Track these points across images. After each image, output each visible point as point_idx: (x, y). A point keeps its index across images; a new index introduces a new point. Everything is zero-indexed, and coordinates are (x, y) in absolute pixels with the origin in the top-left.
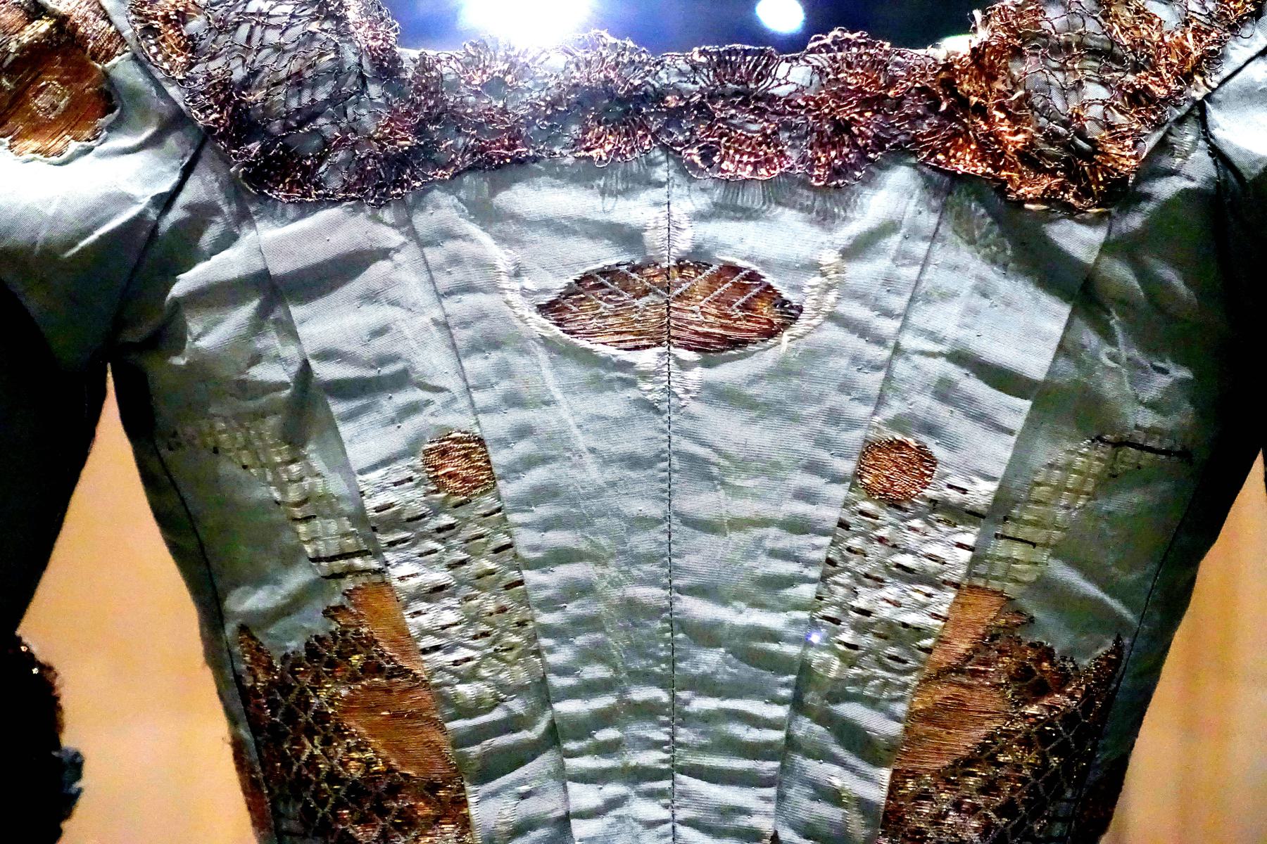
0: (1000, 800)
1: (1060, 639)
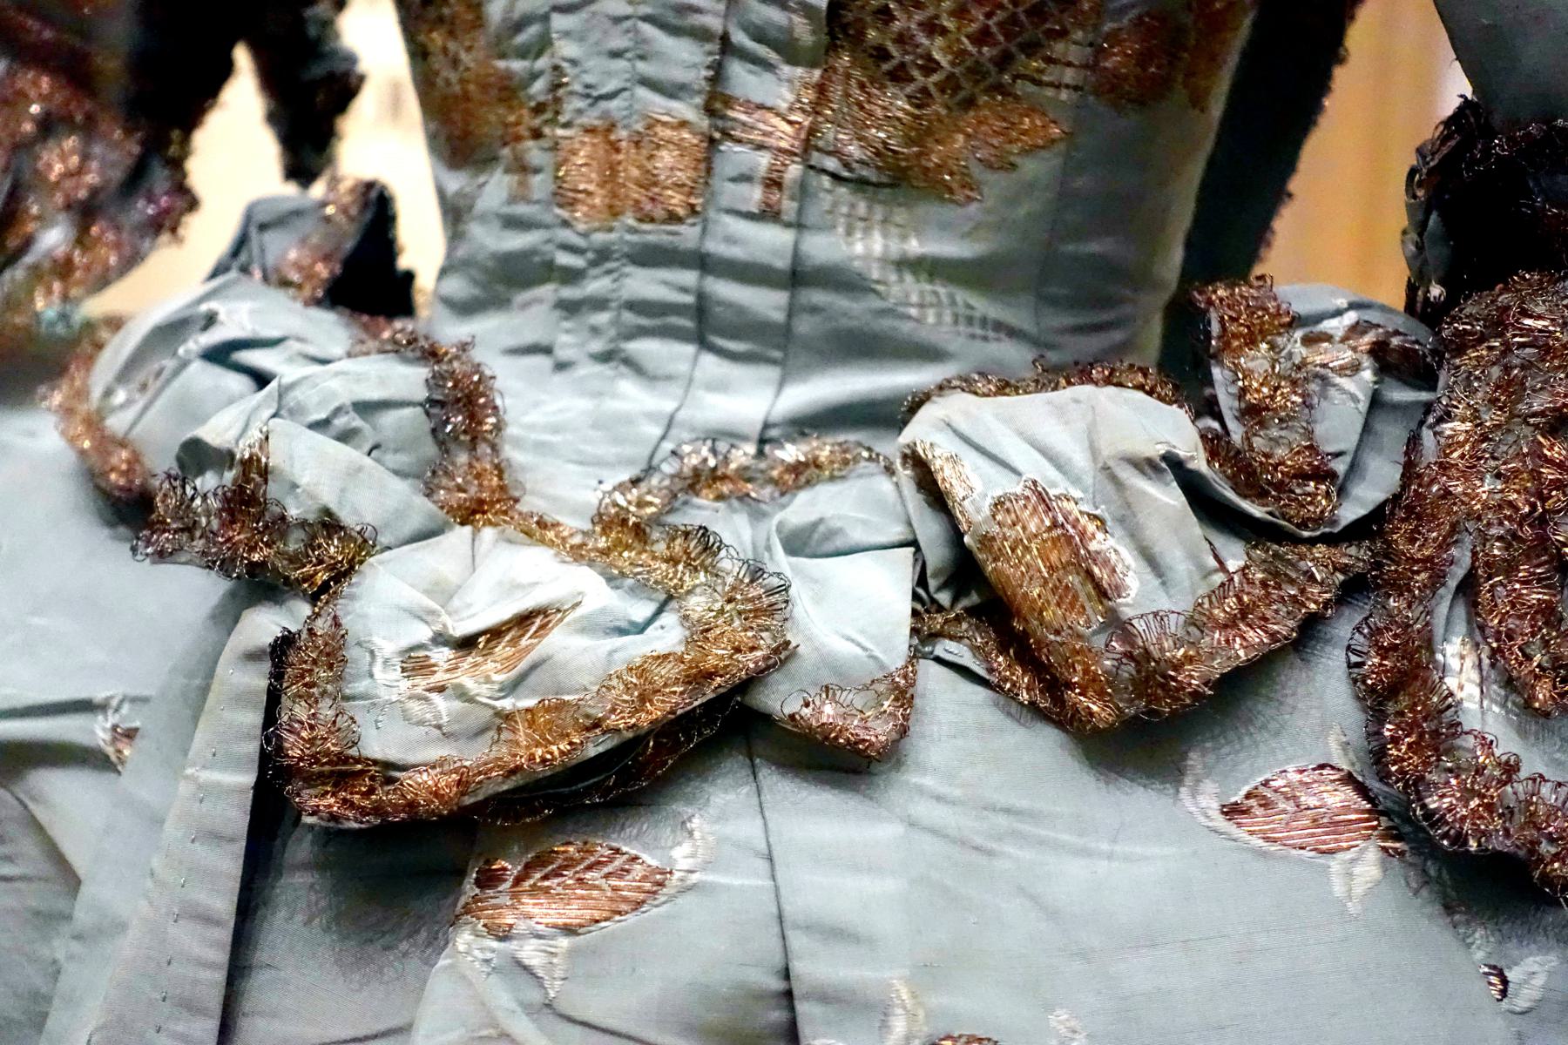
0: (974, 27)
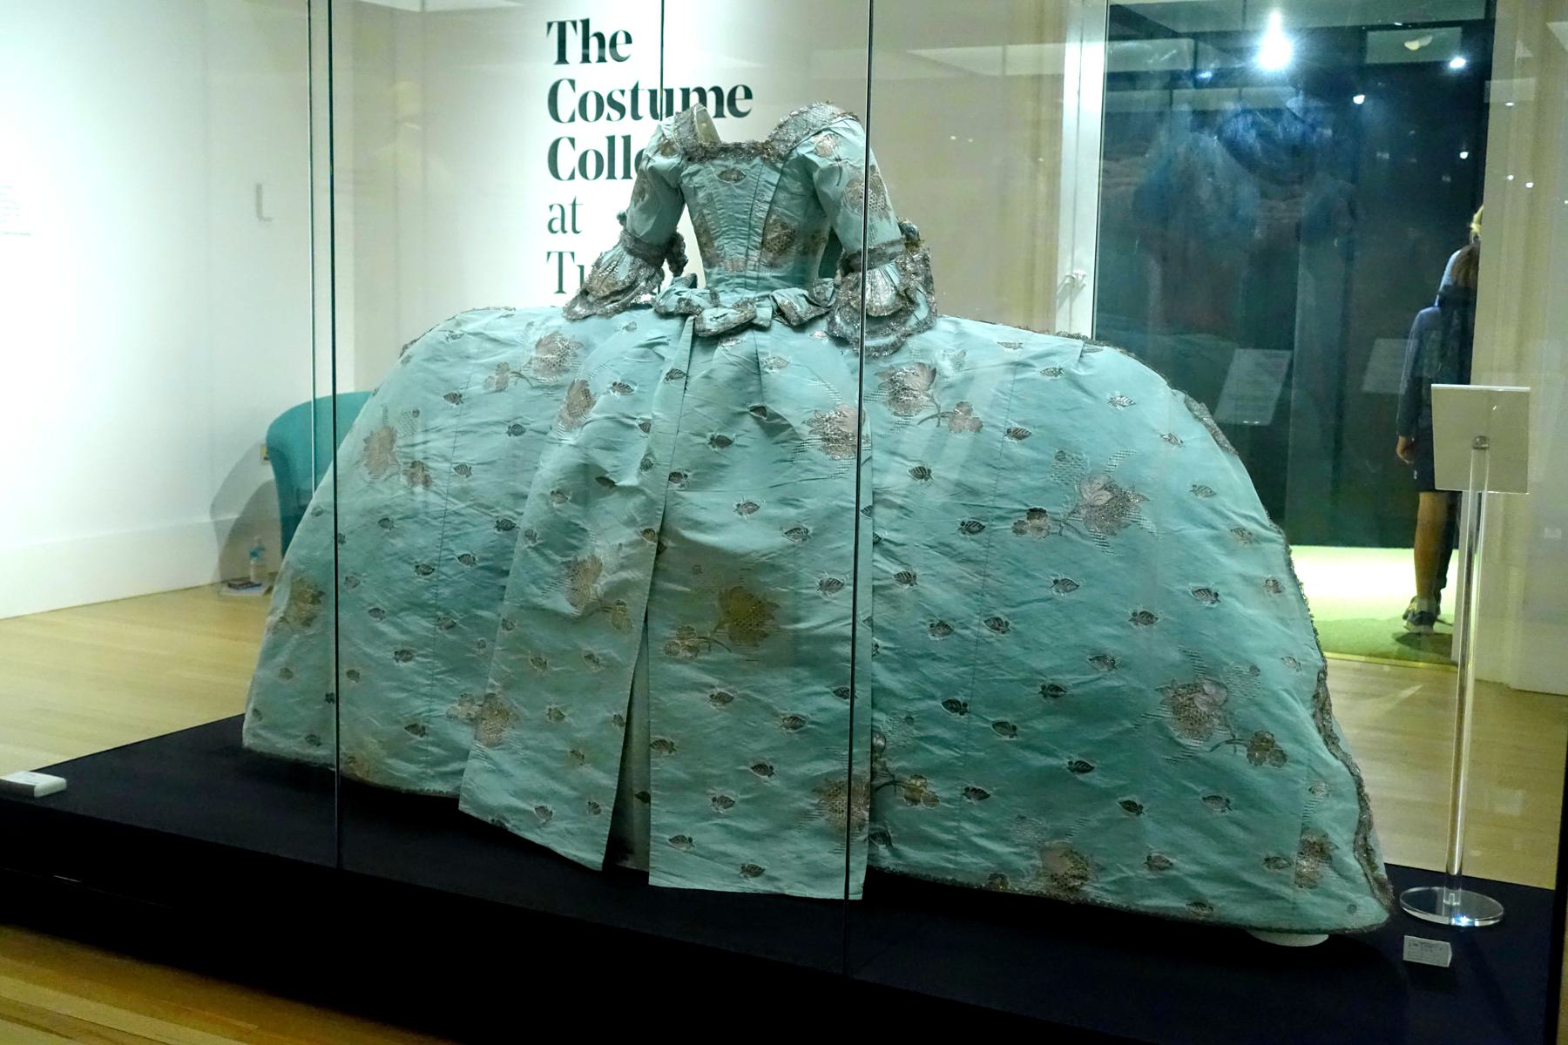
1: (787, 221)
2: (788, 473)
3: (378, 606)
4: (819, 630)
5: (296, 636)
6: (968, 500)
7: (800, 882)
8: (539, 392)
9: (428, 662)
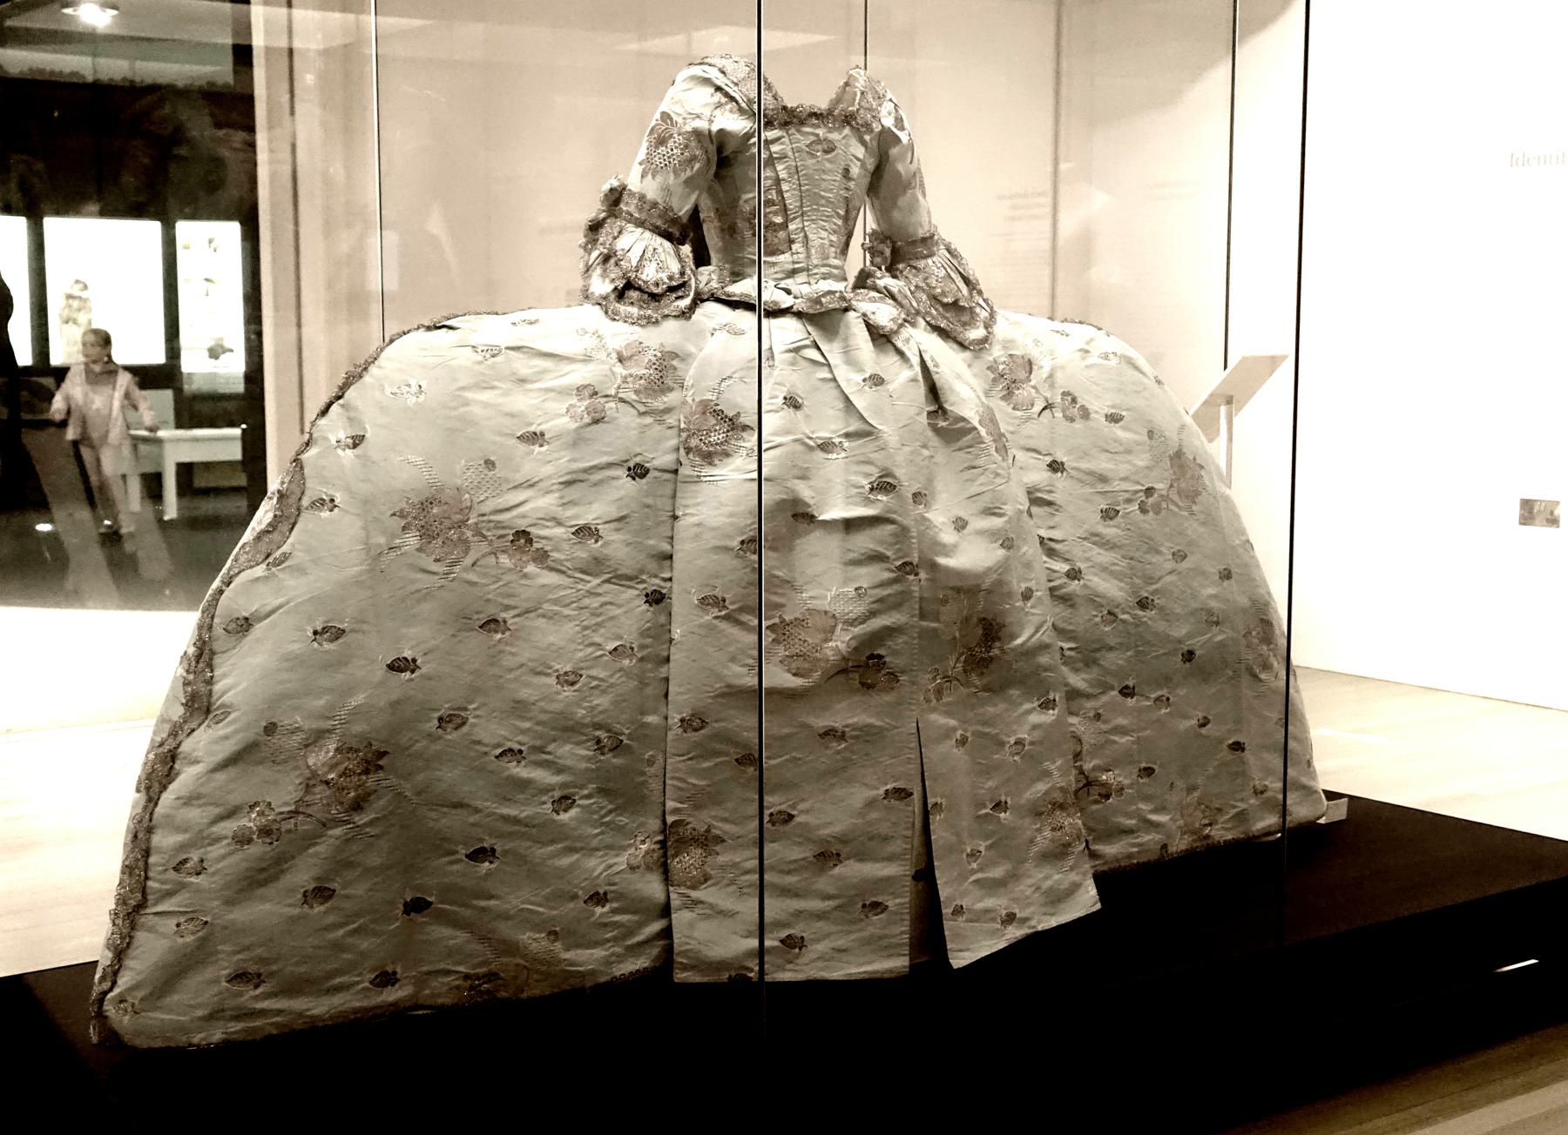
2: (982, 479)
3: (509, 745)
4: (1033, 640)
5: (338, 831)
6: (1100, 487)
7: (1045, 914)
8: (648, 420)
9: (593, 804)
